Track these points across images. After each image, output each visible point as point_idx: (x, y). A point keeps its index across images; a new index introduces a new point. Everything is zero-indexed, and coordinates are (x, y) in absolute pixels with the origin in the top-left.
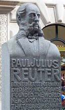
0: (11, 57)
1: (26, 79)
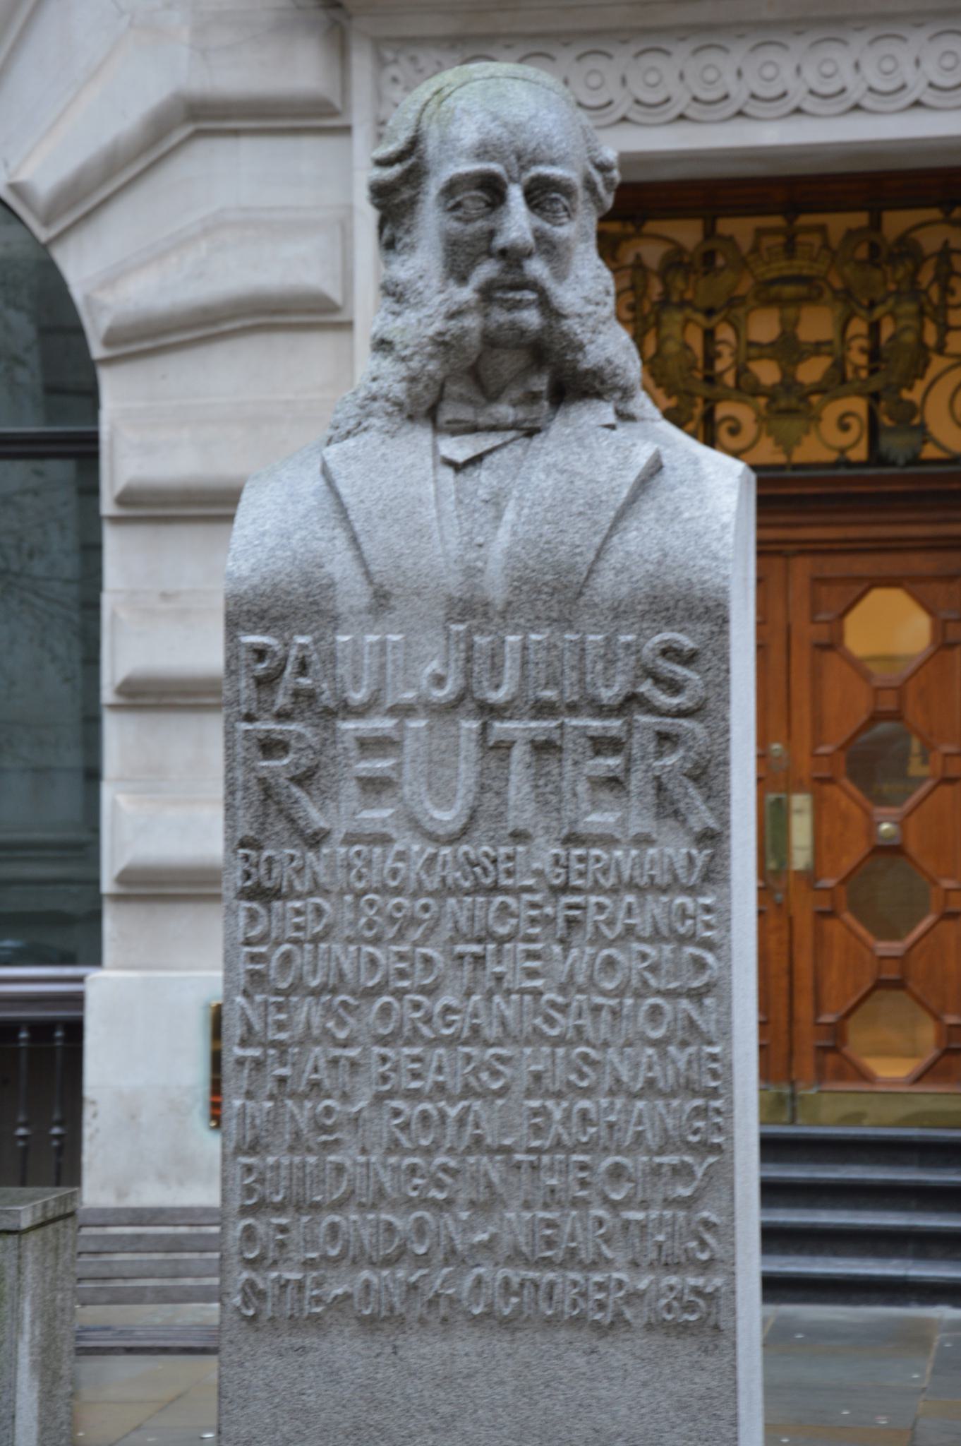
0: (233, 625)
1: (379, 815)
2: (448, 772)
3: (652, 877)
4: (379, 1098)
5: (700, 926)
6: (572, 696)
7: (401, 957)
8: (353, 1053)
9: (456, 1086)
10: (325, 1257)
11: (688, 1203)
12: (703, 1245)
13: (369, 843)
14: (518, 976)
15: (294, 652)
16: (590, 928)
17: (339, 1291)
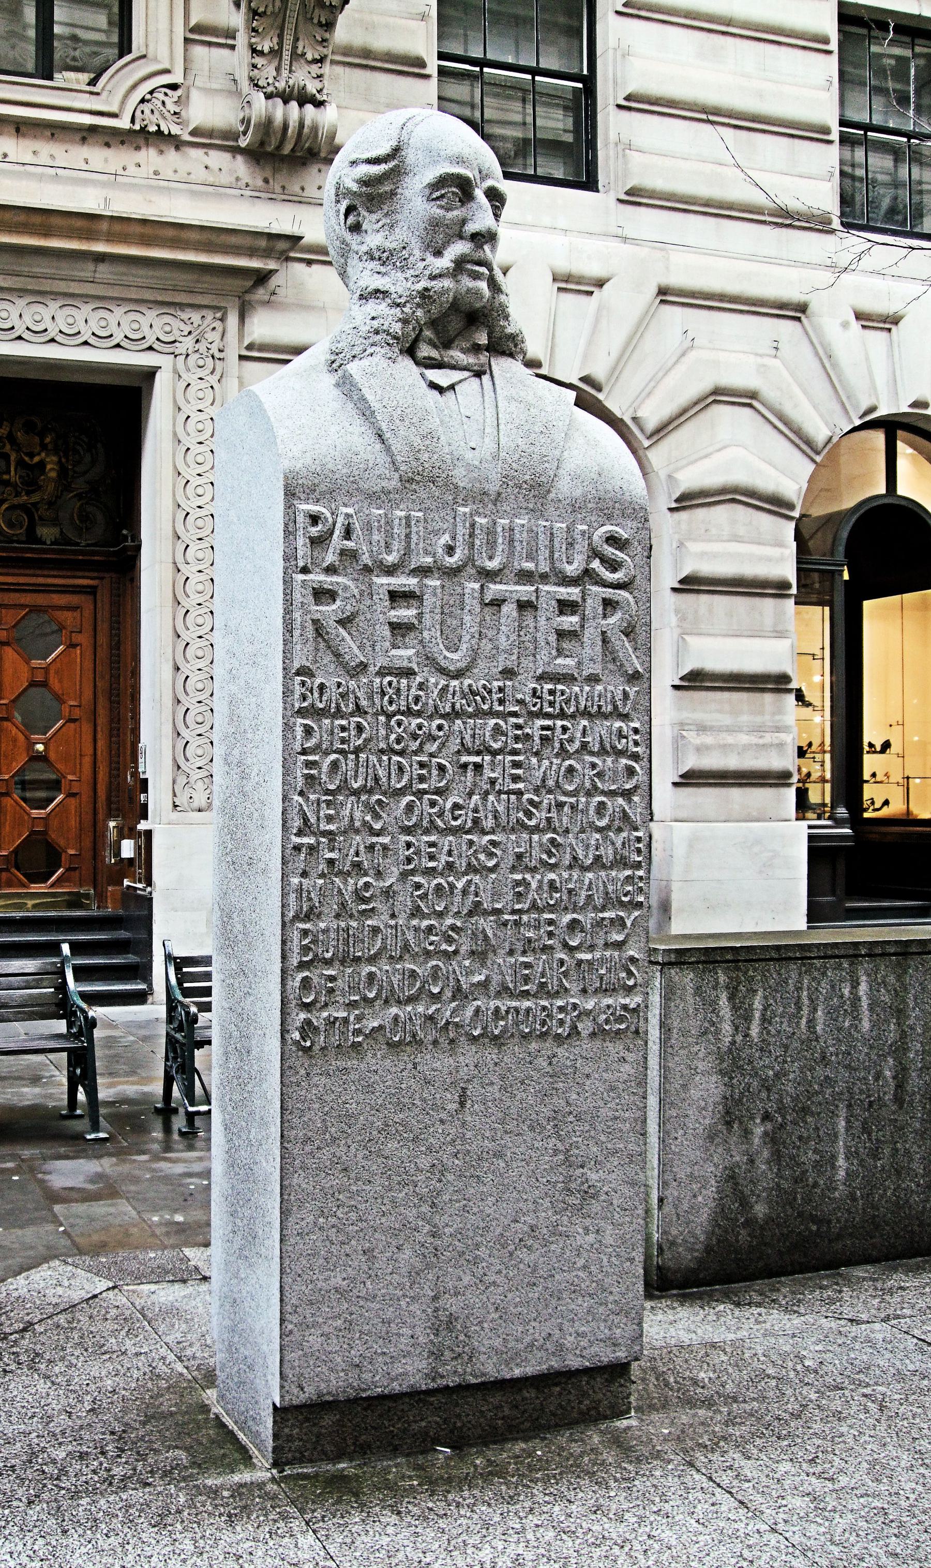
0: (290, 494)
2: (454, 622)
3: (600, 707)
4: (404, 875)
5: (631, 743)
6: (544, 567)
7: (422, 765)
8: (386, 840)
9: (462, 865)
10: (365, 999)
11: (619, 945)
12: (630, 974)
13: (396, 675)
14: (507, 780)
15: (340, 520)
16: (557, 745)
17: (376, 1024)
